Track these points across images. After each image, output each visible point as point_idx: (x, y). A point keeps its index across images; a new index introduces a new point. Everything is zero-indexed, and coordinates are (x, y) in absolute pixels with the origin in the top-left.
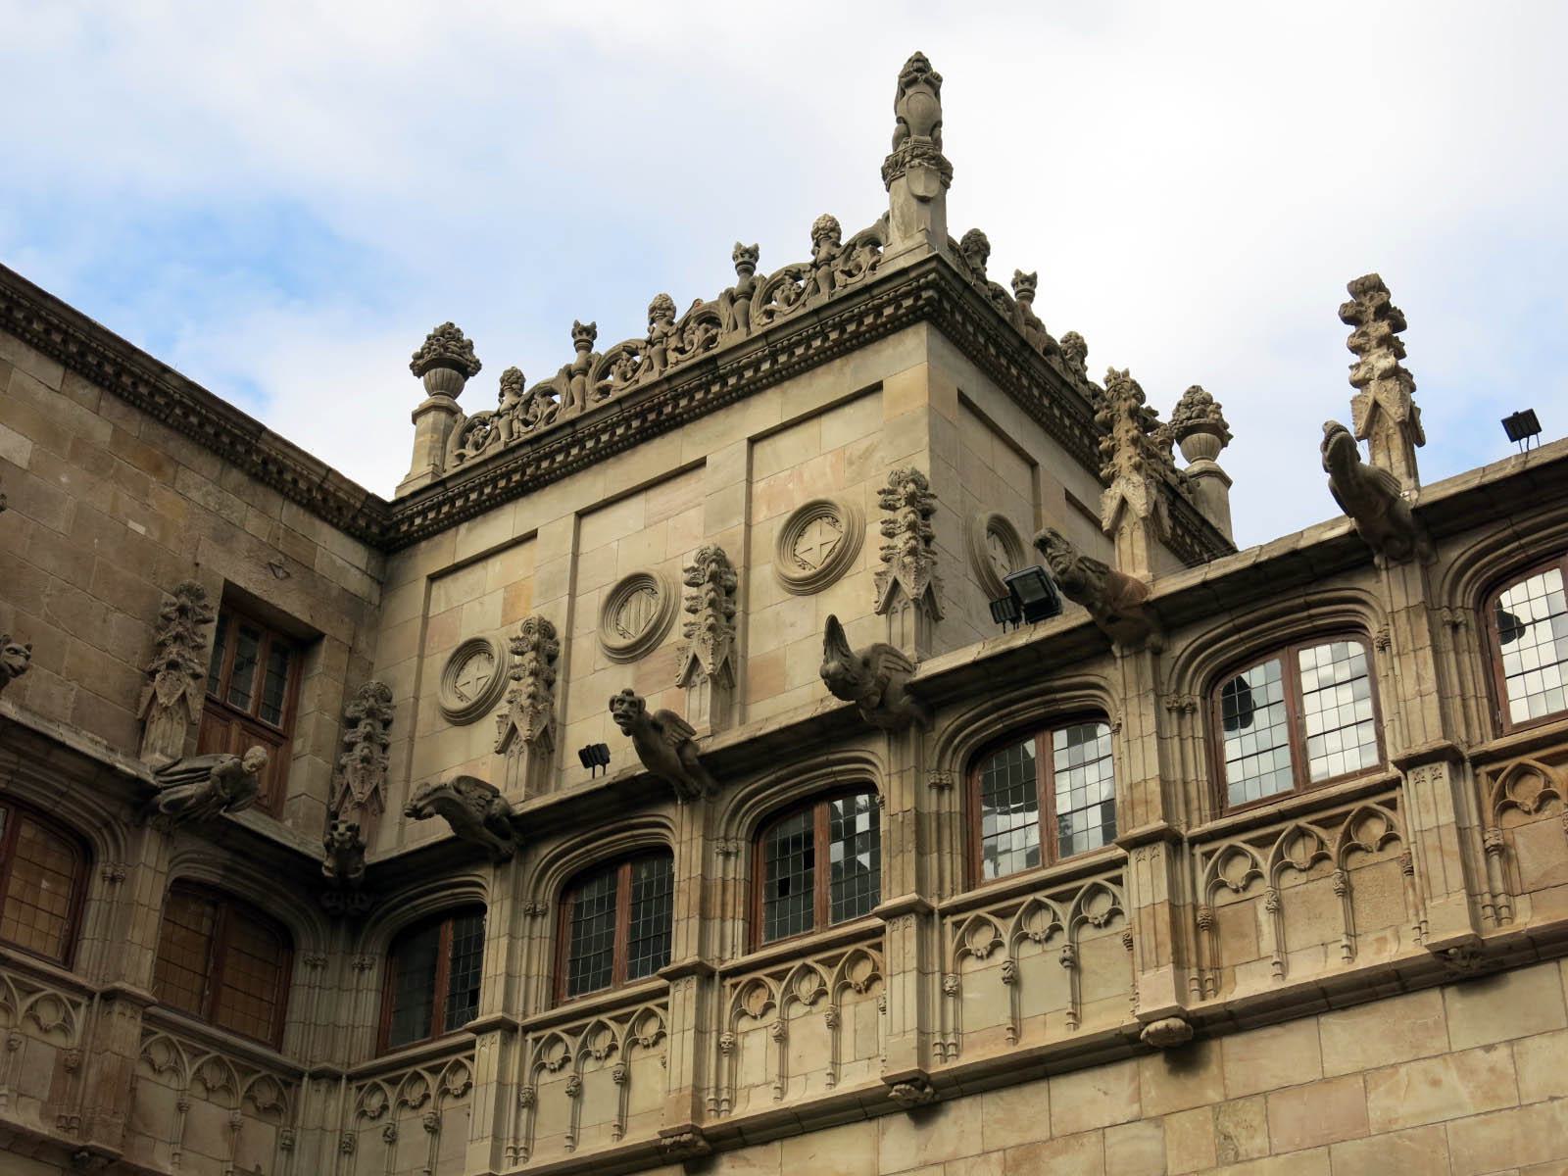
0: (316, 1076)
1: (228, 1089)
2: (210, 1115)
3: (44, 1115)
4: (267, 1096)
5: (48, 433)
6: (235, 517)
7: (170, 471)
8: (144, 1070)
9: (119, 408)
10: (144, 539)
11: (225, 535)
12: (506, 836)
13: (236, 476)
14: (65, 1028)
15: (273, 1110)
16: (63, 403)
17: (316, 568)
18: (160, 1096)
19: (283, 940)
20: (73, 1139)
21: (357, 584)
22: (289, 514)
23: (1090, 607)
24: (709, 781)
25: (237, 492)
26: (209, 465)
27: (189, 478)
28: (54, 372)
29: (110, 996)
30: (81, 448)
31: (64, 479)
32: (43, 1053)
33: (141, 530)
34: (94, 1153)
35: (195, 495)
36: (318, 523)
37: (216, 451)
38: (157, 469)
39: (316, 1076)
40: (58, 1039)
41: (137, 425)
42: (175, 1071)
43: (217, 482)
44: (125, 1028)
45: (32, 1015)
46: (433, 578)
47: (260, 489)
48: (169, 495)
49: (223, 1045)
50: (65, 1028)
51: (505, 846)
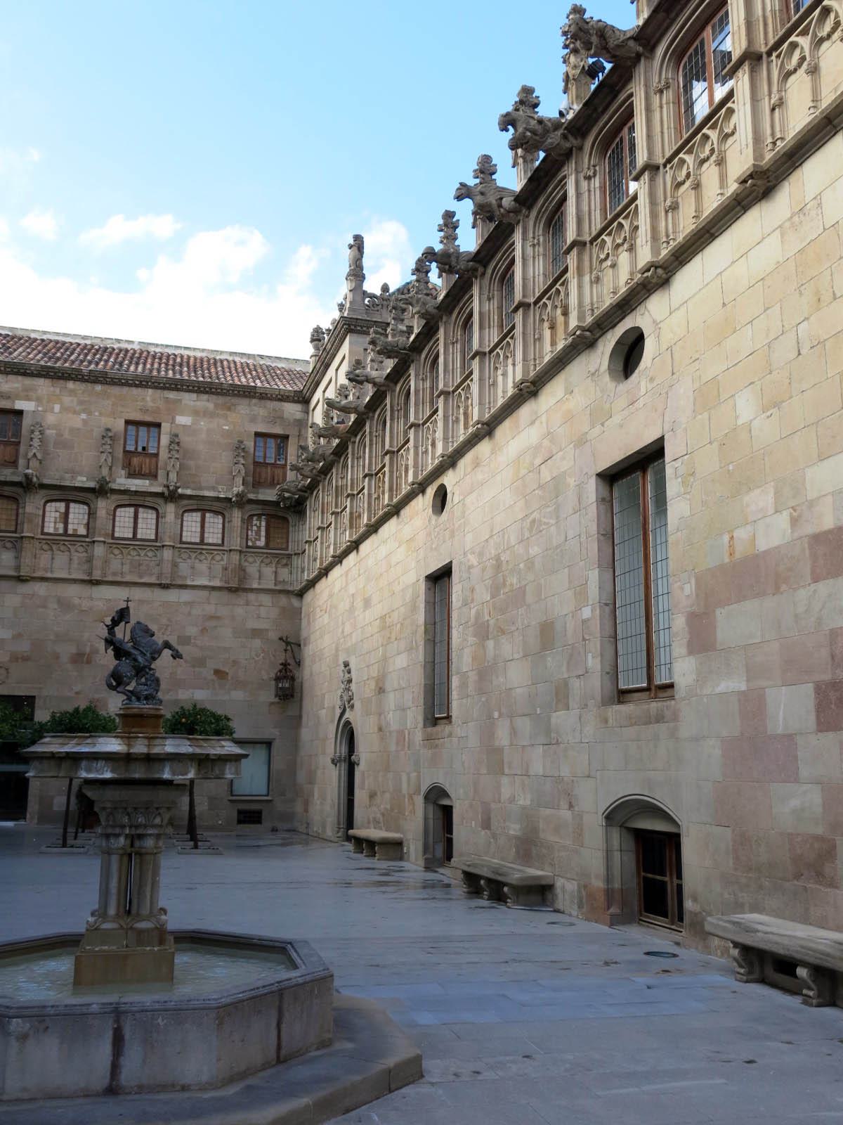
0: (295, 554)
1: (271, 563)
2: (268, 571)
3: (221, 580)
4: (284, 561)
5: (196, 413)
6: (255, 413)
7: (233, 407)
8: (246, 564)
9: (214, 397)
10: (228, 430)
11: (253, 419)
12: (306, 492)
13: (254, 401)
14: (222, 560)
15: (286, 565)
16: (198, 403)
17: (285, 416)
18: (252, 569)
19: (286, 520)
20: (227, 585)
21: (299, 416)
22: (272, 405)
23: (338, 438)
24: (323, 476)
25: (255, 405)
26: (246, 401)
27: (239, 408)
28: (194, 396)
29: (230, 550)
30: (206, 413)
31: (202, 423)
32: (218, 568)
33: (227, 428)
34: (231, 587)
35: (242, 412)
36: (283, 403)
37: (246, 396)
38: (229, 409)
39: (295, 554)
40: (222, 563)
41: (221, 400)
42: (255, 561)
43: (249, 405)
44: (235, 557)
45: (213, 558)
46: (313, 410)
47: (263, 401)
48: (234, 415)
49: (267, 553)
50: (222, 560)
51: (306, 495)
